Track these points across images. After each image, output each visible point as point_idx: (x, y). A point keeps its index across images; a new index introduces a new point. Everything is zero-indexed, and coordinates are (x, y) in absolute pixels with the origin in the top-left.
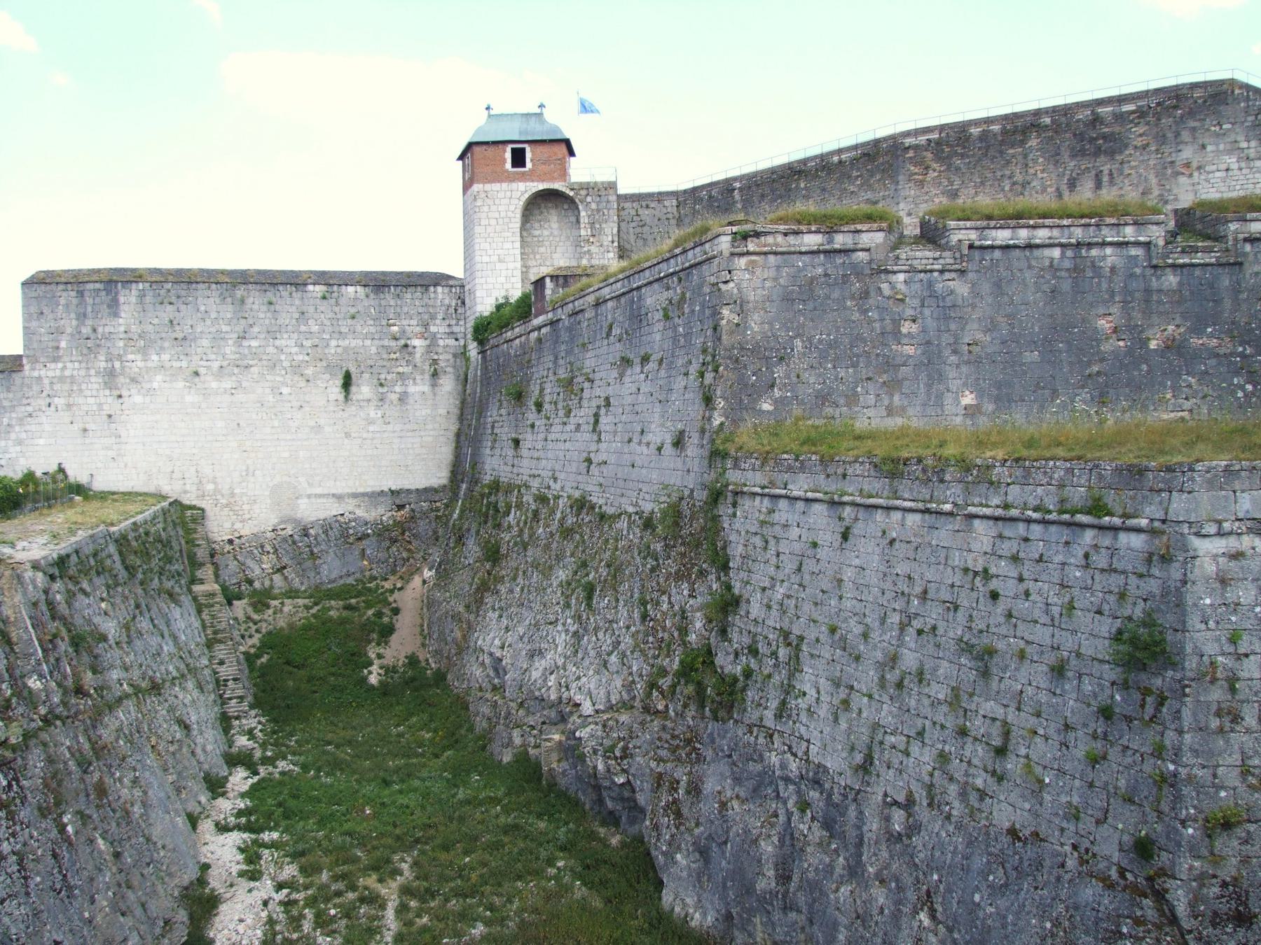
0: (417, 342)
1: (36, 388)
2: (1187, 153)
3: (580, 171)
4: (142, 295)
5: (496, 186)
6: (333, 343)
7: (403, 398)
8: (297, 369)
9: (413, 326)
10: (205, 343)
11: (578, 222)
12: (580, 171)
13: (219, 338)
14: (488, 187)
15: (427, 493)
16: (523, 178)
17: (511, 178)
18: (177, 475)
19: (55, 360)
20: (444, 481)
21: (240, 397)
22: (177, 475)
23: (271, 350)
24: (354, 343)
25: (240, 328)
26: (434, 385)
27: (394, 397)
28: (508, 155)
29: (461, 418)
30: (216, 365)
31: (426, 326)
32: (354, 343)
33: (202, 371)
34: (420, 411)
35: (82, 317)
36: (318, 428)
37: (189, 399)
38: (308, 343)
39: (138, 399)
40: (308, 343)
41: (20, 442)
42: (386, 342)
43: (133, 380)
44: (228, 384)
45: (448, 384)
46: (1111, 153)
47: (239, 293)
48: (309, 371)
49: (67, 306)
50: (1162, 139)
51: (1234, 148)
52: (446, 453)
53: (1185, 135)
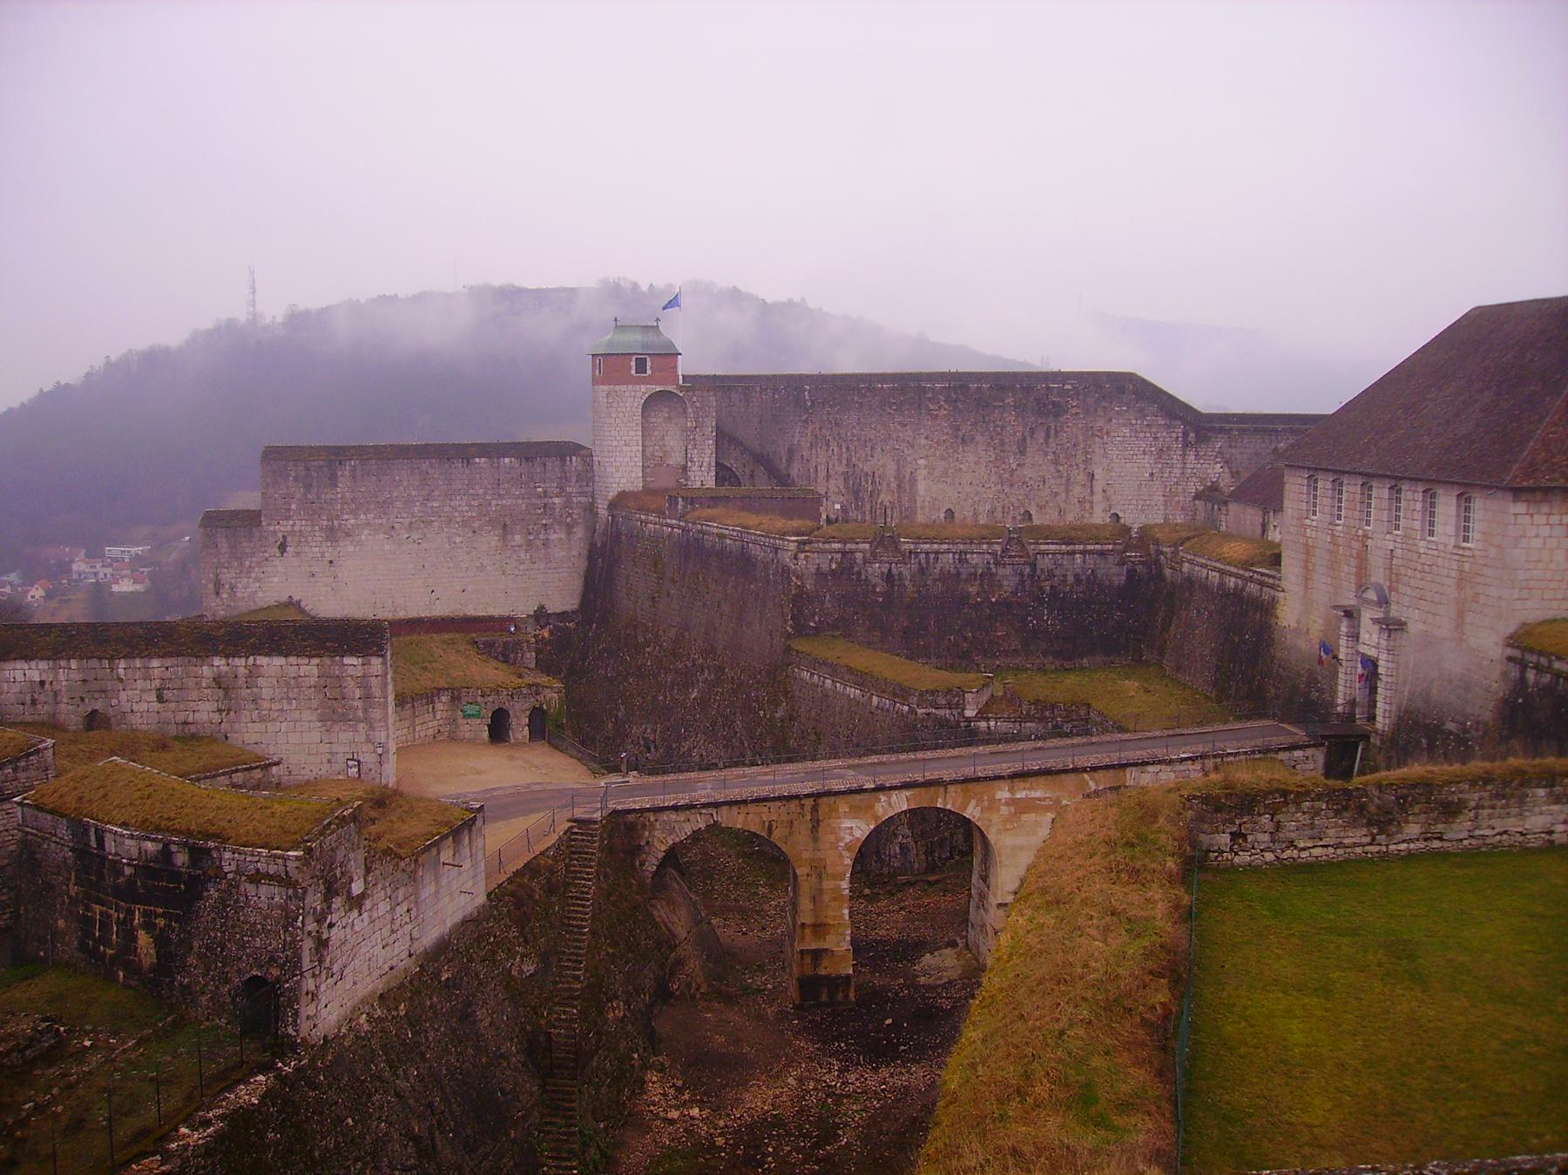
0: (557, 500)
1: (272, 540)
2: (1100, 423)
3: (684, 367)
4: (354, 470)
5: (624, 387)
6: (494, 502)
7: (546, 543)
8: (465, 523)
9: (553, 487)
10: (399, 504)
11: (685, 412)
12: (684, 367)
13: (409, 502)
14: (617, 388)
15: (563, 615)
16: (645, 381)
17: (638, 382)
18: (379, 604)
19: (287, 518)
20: (575, 607)
21: (425, 545)
22: (379, 604)
23: (447, 509)
24: (509, 502)
25: (424, 493)
26: (569, 533)
27: (538, 543)
28: (633, 364)
29: (590, 558)
30: (407, 521)
31: (562, 489)
32: (509, 502)
33: (397, 526)
34: (559, 553)
35: (308, 487)
36: (482, 568)
37: (387, 547)
38: (475, 503)
39: (351, 548)
40: (475, 503)
41: (258, 580)
42: (534, 501)
43: (348, 535)
44: (415, 536)
45: (579, 532)
46: (1057, 415)
47: (425, 465)
48: (476, 525)
49: (296, 479)
50: (1087, 411)
51: (1128, 424)
52: (577, 585)
53: (1100, 412)
